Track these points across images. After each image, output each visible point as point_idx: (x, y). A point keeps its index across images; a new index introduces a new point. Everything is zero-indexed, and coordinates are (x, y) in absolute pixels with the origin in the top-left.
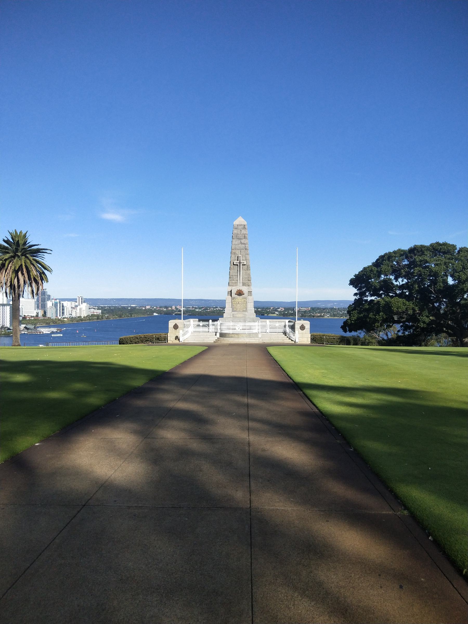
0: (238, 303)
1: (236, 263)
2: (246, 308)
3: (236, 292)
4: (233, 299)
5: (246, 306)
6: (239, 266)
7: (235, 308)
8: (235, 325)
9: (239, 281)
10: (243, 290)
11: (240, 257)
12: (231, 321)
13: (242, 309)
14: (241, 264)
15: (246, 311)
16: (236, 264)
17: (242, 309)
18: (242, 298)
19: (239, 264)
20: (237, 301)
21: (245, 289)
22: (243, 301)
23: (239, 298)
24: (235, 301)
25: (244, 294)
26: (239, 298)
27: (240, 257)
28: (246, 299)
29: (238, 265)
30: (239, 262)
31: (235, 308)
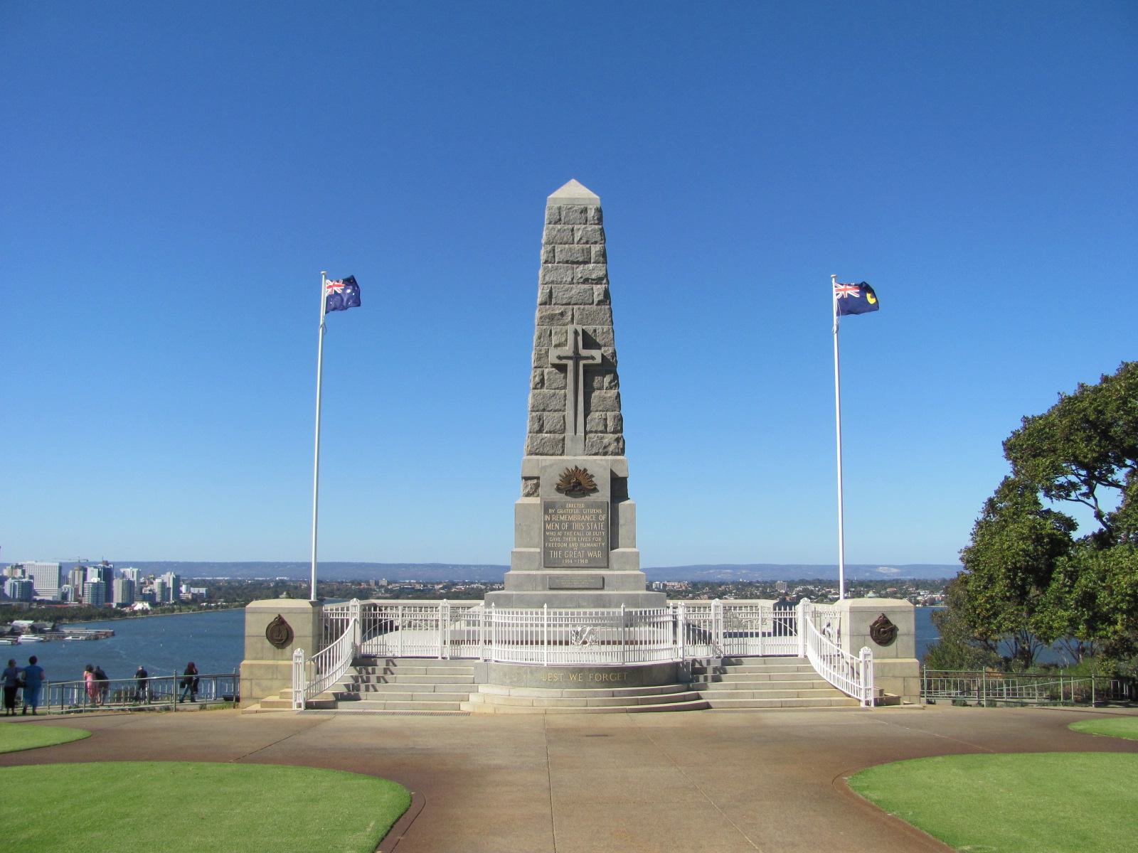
0: (570, 528)
1: (560, 358)
7: (554, 549)
8: (754, 631)
9: (569, 433)
10: (589, 472)
12: (545, 606)
14: (582, 363)
16: (557, 361)
18: (589, 506)
19: (570, 363)
21: (600, 467)
23: (575, 506)
24: (555, 518)
25: (595, 490)
27: (576, 333)
29: (566, 366)
30: (568, 350)
31: (554, 549)
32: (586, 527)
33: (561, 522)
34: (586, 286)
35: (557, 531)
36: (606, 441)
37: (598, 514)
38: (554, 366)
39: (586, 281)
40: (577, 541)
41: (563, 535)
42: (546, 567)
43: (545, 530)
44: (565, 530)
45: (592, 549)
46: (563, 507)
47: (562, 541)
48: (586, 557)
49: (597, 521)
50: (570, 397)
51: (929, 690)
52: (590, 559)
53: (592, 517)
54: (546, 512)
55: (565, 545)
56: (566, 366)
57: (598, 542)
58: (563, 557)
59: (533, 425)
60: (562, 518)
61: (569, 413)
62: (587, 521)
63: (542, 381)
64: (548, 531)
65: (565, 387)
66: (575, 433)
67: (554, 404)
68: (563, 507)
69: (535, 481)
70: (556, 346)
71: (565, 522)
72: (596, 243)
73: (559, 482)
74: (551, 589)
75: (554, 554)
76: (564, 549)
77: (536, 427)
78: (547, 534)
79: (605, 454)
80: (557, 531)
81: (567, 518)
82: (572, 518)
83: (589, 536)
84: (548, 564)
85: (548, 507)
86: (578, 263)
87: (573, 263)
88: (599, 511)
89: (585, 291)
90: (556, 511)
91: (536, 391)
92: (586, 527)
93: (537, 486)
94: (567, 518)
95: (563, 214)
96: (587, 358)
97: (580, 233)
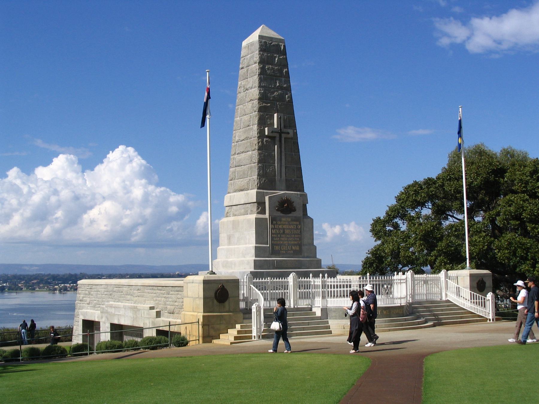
0: (284, 232)
2: (300, 245)
5: (301, 239)
6: (277, 139)
7: (276, 245)
10: (292, 200)
17: (291, 247)
18: (292, 220)
19: (277, 135)
20: (280, 227)
25: (294, 210)
26: (283, 219)
28: (300, 224)
31: (276, 245)
32: (292, 232)
33: (279, 229)
35: (277, 234)
37: (297, 225)
40: (287, 240)
41: (280, 236)
44: (282, 234)
45: (294, 245)
46: (280, 221)
49: (297, 229)
51: (204, 342)
53: (294, 227)
55: (282, 242)
57: (297, 241)
58: (281, 250)
59: (260, 171)
60: (280, 227)
62: (292, 229)
64: (273, 234)
66: (281, 177)
68: (280, 221)
71: (281, 229)
73: (278, 205)
75: (277, 248)
78: (273, 236)
80: (277, 234)
81: (282, 227)
82: (285, 227)
83: (293, 237)
85: (273, 219)
88: (298, 223)
90: (277, 223)
91: (260, 152)
92: (292, 232)
94: (282, 227)
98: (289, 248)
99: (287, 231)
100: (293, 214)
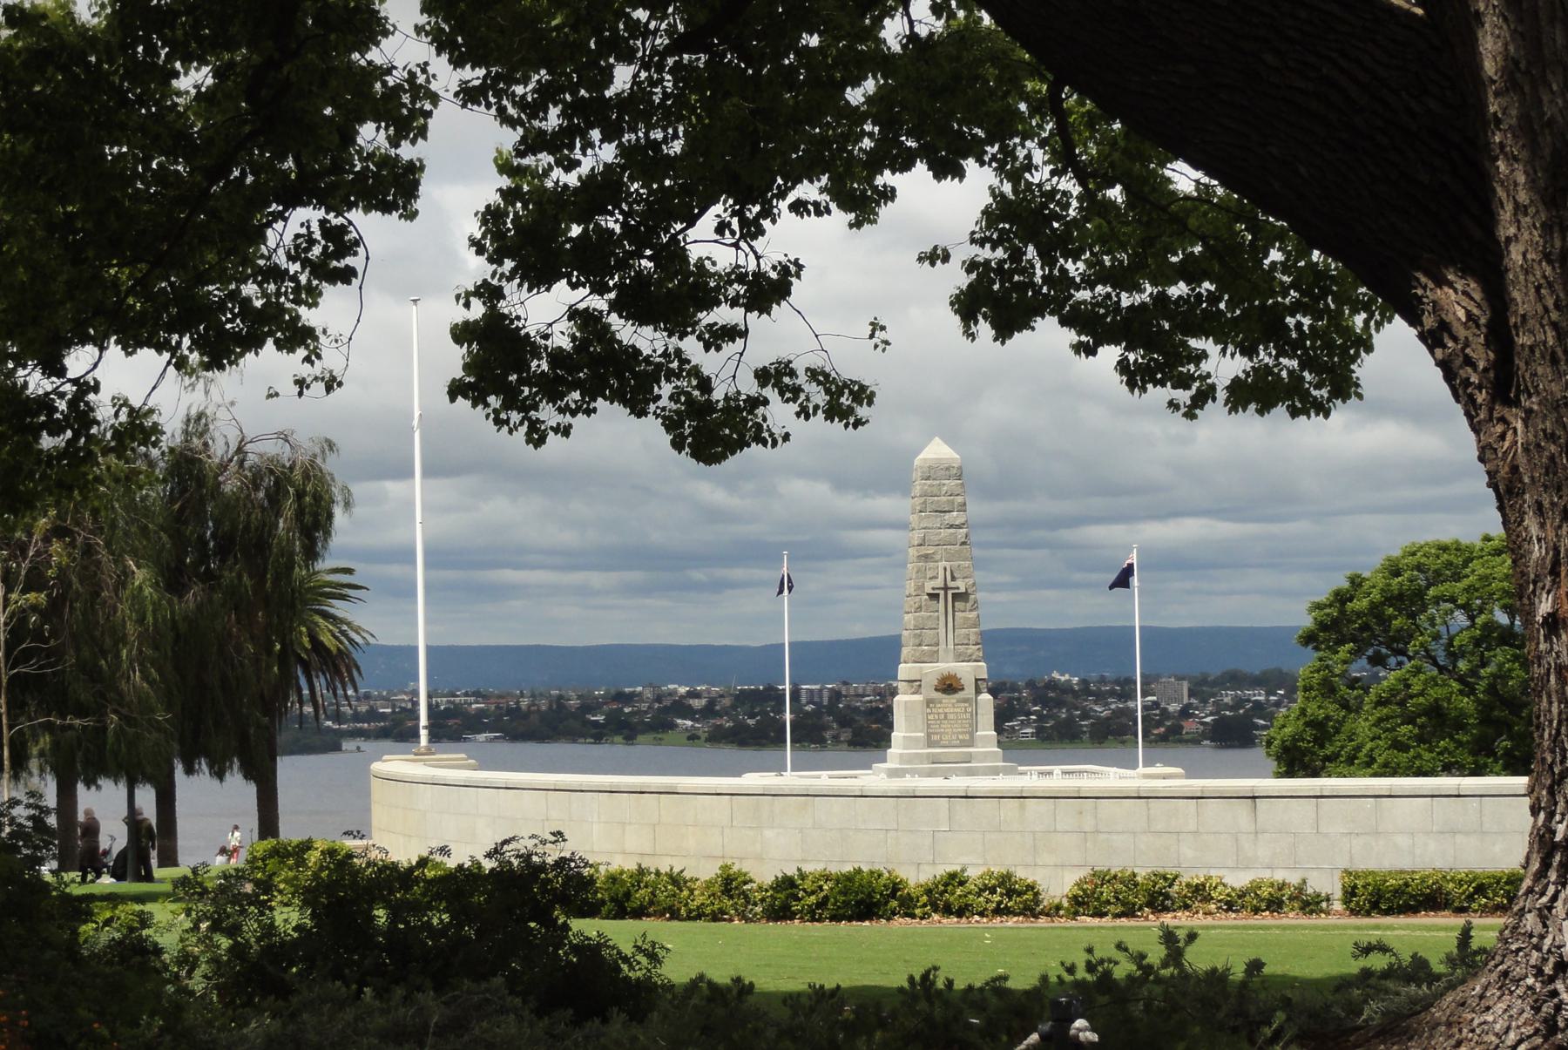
0: (946, 718)
1: (933, 589)
2: (972, 734)
3: (936, 682)
4: (928, 706)
9: (942, 647)
10: (958, 676)
11: (945, 569)
13: (958, 738)
14: (950, 593)
15: (971, 743)
16: (932, 592)
18: (958, 701)
22: (959, 710)
25: (963, 689)
27: (945, 569)
29: (938, 594)
30: (939, 583)
34: (952, 530)
36: (969, 651)
38: (928, 594)
39: (951, 526)
42: (929, 746)
43: (928, 720)
47: (940, 728)
48: (958, 738)
49: (966, 712)
50: (942, 618)
52: (961, 741)
54: (928, 706)
56: (938, 594)
60: (941, 711)
61: (942, 630)
63: (920, 607)
65: (937, 611)
67: (930, 624)
68: (941, 703)
69: (918, 683)
70: (930, 578)
72: (958, 495)
74: (934, 763)
75: (935, 738)
76: (941, 733)
77: (917, 642)
79: (969, 661)
84: (930, 744)
85: (929, 702)
86: (945, 512)
87: (941, 512)
88: (967, 705)
89: (951, 534)
93: (920, 686)
95: (932, 471)
96: (952, 588)
97: (945, 488)
98: (954, 737)
99: (951, 716)
100: (960, 695)
